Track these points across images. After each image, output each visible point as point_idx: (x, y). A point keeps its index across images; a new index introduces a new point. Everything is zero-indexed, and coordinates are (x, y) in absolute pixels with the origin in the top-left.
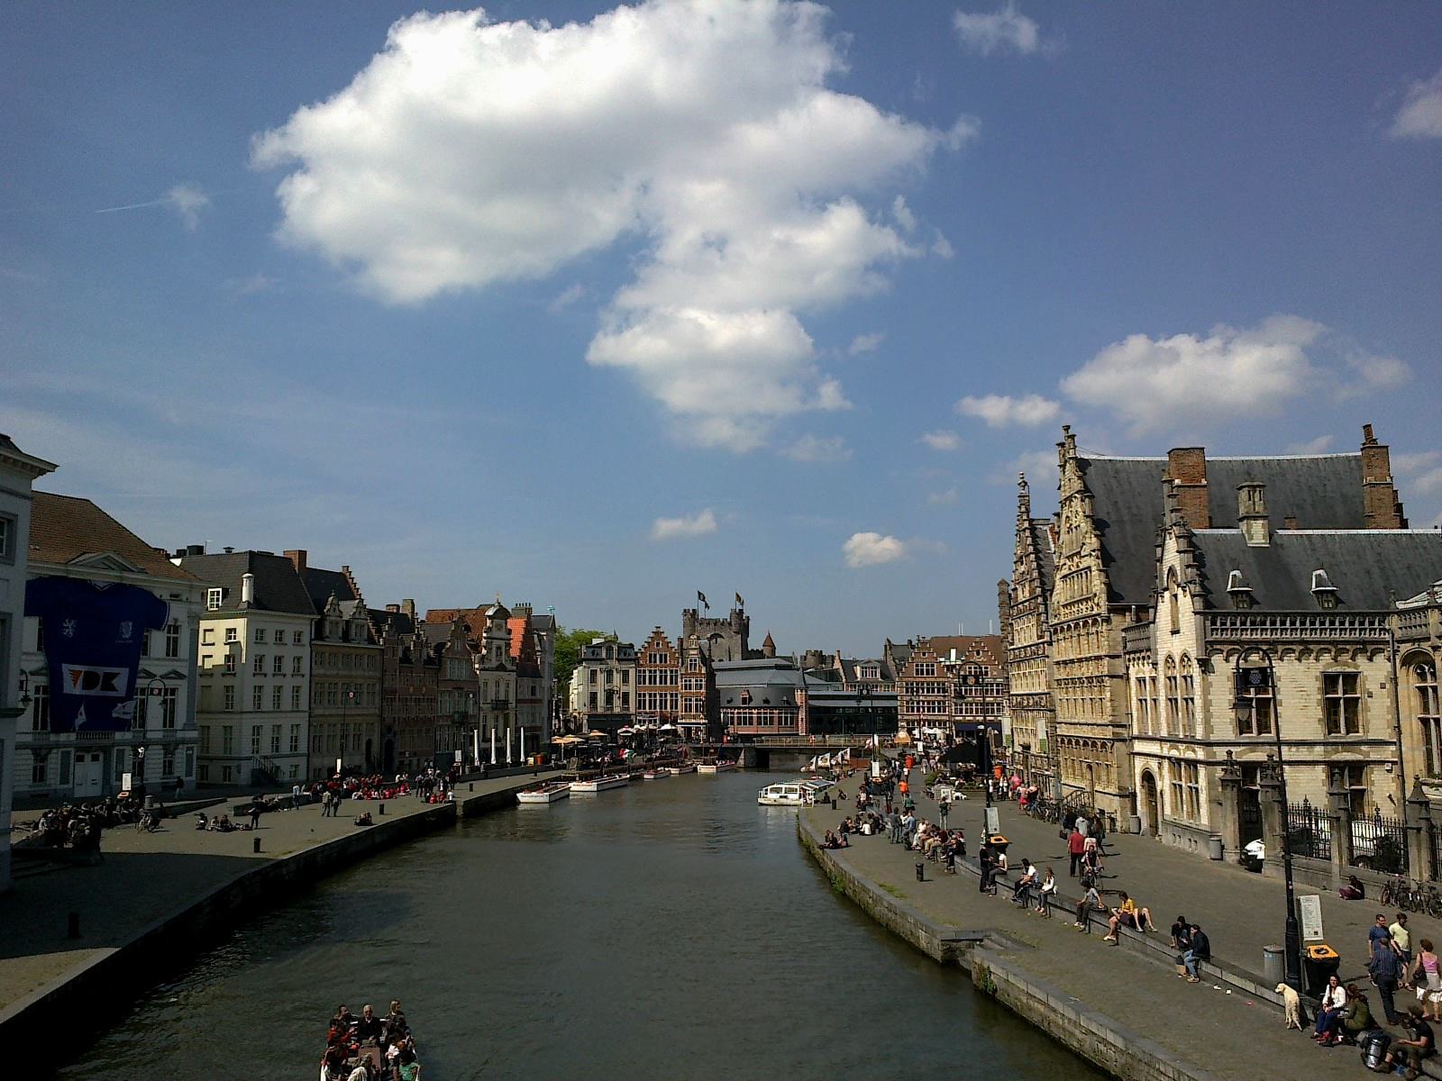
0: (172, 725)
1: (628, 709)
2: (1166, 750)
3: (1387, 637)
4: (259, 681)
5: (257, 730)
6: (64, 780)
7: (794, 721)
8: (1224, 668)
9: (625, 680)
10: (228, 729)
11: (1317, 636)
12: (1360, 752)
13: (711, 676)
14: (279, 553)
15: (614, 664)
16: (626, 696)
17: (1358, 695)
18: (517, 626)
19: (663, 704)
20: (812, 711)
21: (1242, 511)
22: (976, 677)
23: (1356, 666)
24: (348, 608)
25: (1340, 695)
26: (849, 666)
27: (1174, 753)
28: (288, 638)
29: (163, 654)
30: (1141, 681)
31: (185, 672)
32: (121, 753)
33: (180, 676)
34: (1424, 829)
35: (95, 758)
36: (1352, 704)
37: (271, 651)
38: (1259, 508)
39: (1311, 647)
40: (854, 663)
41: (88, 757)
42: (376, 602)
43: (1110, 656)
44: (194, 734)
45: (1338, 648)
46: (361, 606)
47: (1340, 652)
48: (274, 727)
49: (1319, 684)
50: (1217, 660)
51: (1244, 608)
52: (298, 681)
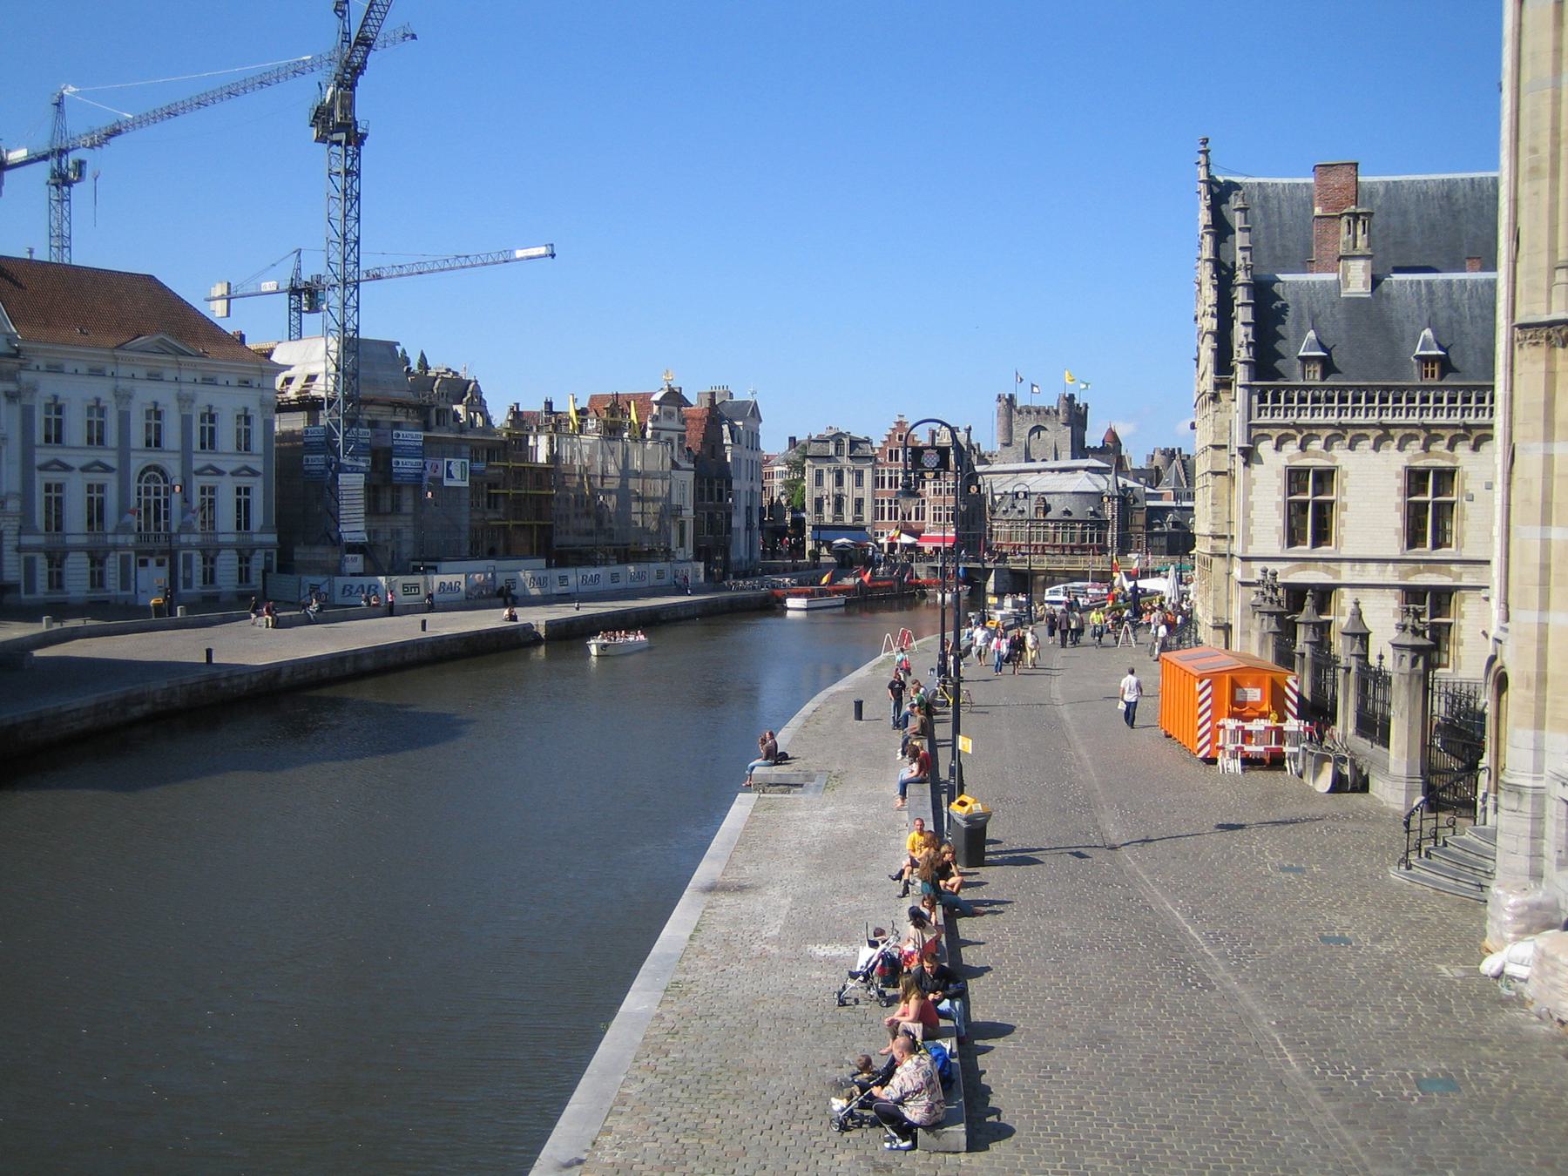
0: (247, 526)
1: (861, 519)
6: (125, 585)
8: (1275, 461)
11: (1401, 419)
12: (1449, 573)
17: (1454, 498)
23: (1454, 459)
25: (1309, 497)
29: (83, 441)
31: (259, 467)
33: (254, 473)
34: (1354, 670)
35: (160, 564)
36: (1444, 511)
38: (1362, 242)
39: (1392, 431)
41: (152, 562)
43: (1214, 447)
47: (1431, 439)
49: (1400, 483)
50: (1265, 448)
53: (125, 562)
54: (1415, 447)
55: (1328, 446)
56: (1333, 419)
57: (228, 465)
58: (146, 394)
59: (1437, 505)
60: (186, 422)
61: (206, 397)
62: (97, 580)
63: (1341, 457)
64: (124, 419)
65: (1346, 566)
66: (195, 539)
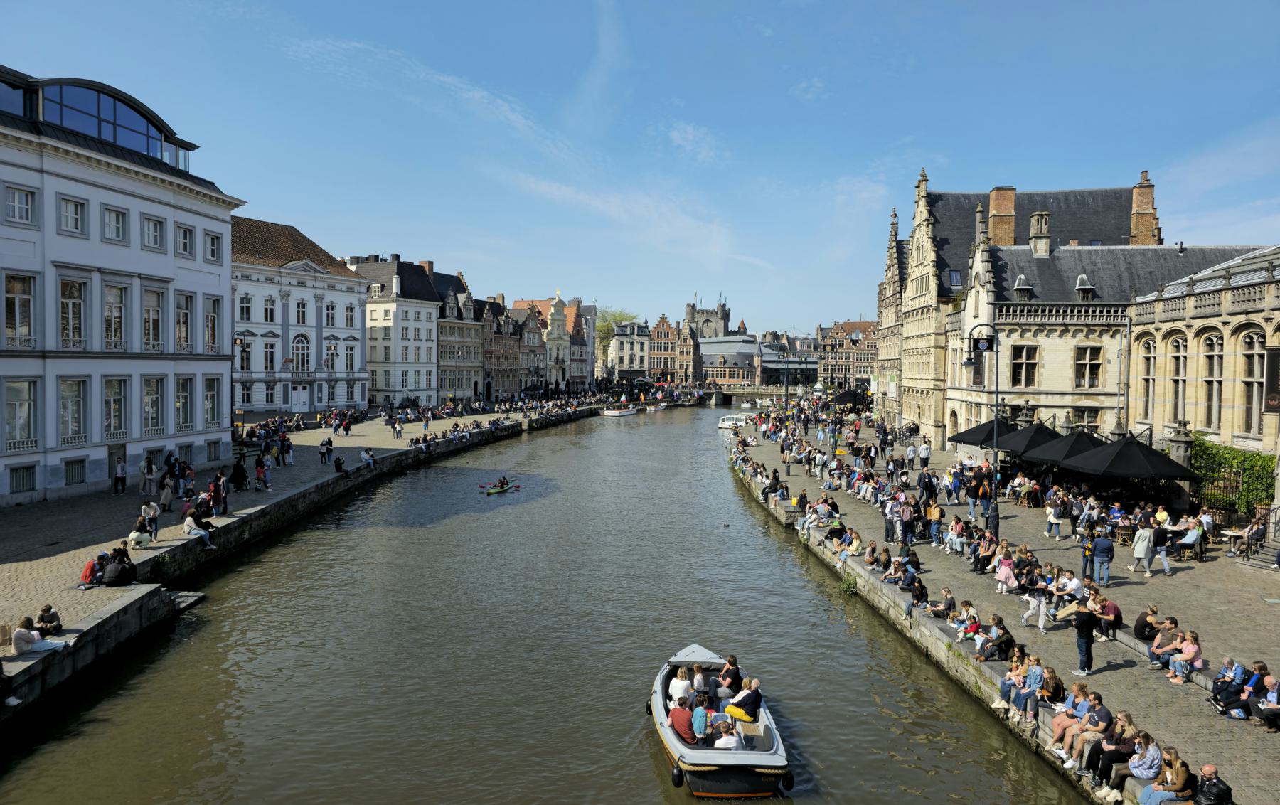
2: (964, 396)
3: (1127, 321)
4: (406, 343)
5: (405, 374)
6: (286, 401)
7: (753, 376)
9: (642, 349)
10: (387, 372)
11: (1075, 321)
13: (697, 346)
14: (416, 263)
15: (635, 337)
16: (642, 359)
18: (570, 314)
19: (666, 363)
20: (765, 370)
21: (1032, 233)
22: (833, 346)
24: (462, 297)
26: (792, 341)
27: (969, 399)
28: (423, 317)
30: (955, 350)
32: (320, 386)
35: (304, 389)
36: (1095, 369)
37: (412, 325)
38: (1045, 229)
40: (796, 339)
41: (300, 388)
42: (480, 294)
44: (365, 375)
45: (1090, 329)
46: (469, 298)
47: (1091, 331)
48: (415, 371)
49: (1072, 354)
51: (1025, 300)
52: (430, 344)
53: (286, 387)
54: (1081, 336)
55: (1035, 335)
56: (1038, 321)
57: (342, 335)
58: (297, 294)
59: (1091, 366)
60: (319, 310)
61: (329, 297)
62: (270, 398)
63: (1041, 340)
64: (285, 308)
65: (1043, 397)
66: (325, 375)
